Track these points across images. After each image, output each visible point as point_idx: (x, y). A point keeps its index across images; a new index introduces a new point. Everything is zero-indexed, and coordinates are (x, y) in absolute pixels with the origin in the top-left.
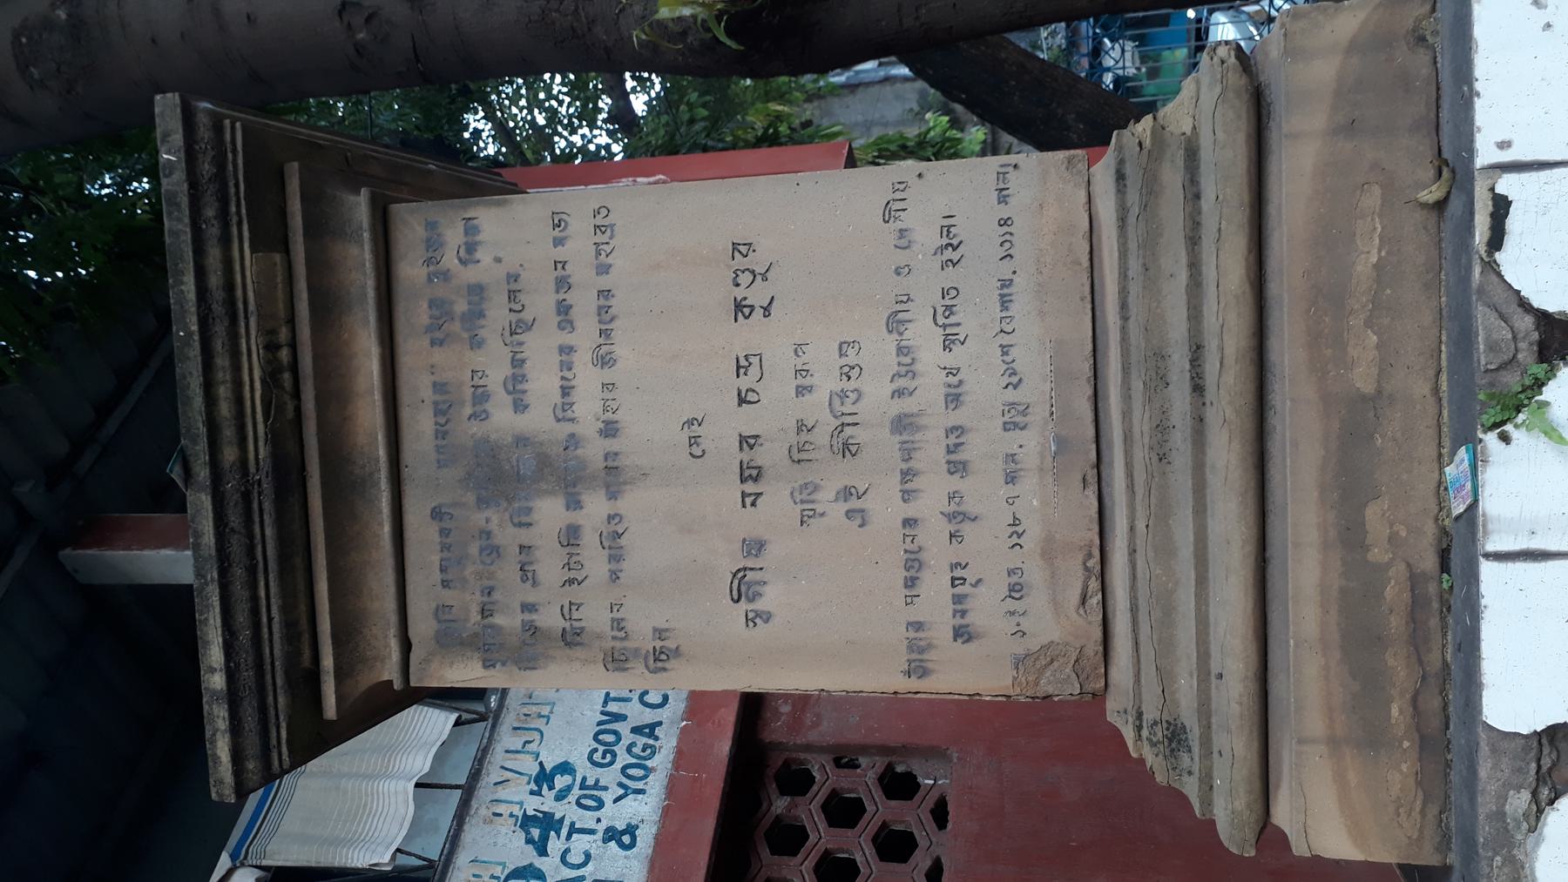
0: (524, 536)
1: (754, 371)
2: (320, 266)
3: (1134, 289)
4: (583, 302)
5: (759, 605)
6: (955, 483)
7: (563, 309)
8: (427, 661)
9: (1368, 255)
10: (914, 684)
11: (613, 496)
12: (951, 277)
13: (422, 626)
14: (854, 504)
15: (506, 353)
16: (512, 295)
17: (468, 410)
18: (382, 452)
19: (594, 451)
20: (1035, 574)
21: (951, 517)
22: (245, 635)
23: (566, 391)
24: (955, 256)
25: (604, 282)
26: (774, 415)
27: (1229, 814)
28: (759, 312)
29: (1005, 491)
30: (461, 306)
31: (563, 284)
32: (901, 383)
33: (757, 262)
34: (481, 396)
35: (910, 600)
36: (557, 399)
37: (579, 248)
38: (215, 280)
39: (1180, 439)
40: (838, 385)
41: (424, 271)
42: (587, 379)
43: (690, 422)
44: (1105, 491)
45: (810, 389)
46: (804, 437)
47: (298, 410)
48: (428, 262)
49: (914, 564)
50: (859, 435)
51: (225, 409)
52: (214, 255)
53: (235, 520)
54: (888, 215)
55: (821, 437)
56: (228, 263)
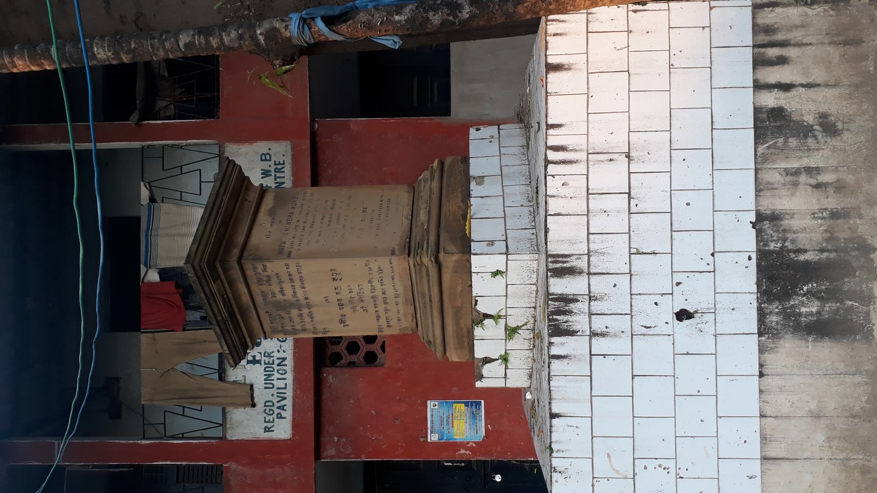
4: (296, 278)
7: (291, 280)
9: (459, 289)
19: (304, 302)
20: (402, 318)
22: (231, 343)
34: (273, 294)
38: (208, 292)
51: (216, 311)
52: (206, 288)
53: (223, 327)
56: (210, 288)
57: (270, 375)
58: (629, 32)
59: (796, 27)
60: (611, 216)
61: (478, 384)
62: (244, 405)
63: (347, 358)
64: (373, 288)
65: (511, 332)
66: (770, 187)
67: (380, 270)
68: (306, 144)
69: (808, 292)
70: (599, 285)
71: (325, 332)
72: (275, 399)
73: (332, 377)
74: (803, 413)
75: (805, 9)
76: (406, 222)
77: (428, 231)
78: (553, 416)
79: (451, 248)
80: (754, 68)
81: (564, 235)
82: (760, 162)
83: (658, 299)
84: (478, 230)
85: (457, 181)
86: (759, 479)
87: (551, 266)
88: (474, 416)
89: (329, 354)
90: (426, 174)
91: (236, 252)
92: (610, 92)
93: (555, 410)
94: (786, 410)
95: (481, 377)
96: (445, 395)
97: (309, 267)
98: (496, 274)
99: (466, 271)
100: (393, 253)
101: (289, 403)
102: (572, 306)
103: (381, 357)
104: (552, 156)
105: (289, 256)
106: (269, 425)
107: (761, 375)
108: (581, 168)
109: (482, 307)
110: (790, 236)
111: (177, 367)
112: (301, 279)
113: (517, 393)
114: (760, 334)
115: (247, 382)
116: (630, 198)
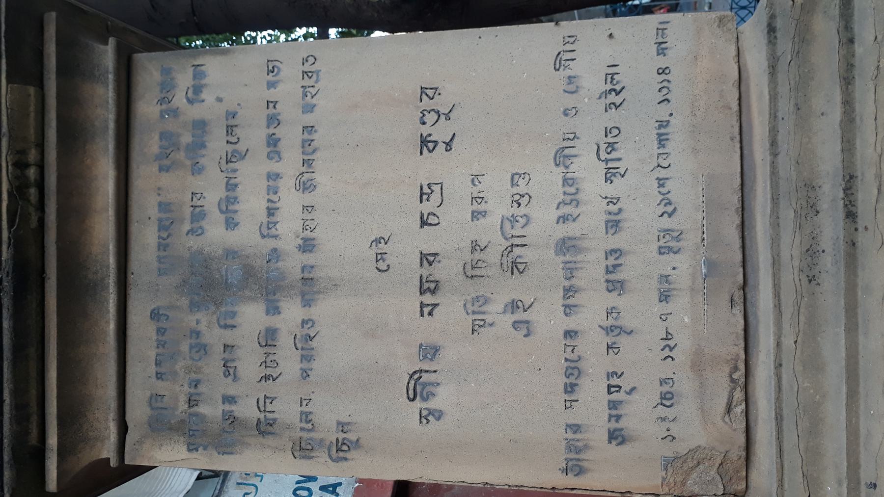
0: (229, 336)
1: (435, 198)
2: (69, 101)
3: (785, 128)
4: (290, 137)
5: (432, 404)
6: (613, 300)
7: (273, 142)
8: (140, 442)
10: (571, 481)
11: (307, 303)
12: (613, 118)
13: (137, 412)
14: (520, 316)
15: (221, 178)
16: (230, 130)
17: (187, 227)
18: (112, 260)
19: (293, 264)
20: (685, 385)
21: (609, 330)
23: (271, 212)
24: (618, 100)
25: (309, 119)
26: (452, 235)
28: (441, 147)
29: (659, 308)
30: (186, 138)
31: (273, 120)
32: (565, 210)
33: (442, 104)
34: (198, 215)
35: (569, 405)
36: (263, 217)
37: (288, 90)
39: (830, 263)
40: (508, 210)
41: (158, 108)
42: (290, 201)
43: (378, 241)
44: (749, 310)
45: (484, 214)
46: (477, 255)
47: (42, 222)
48: (161, 101)
49: (573, 371)
50: (527, 255)
54: (559, 63)
55: (493, 256)
67: (614, 91)
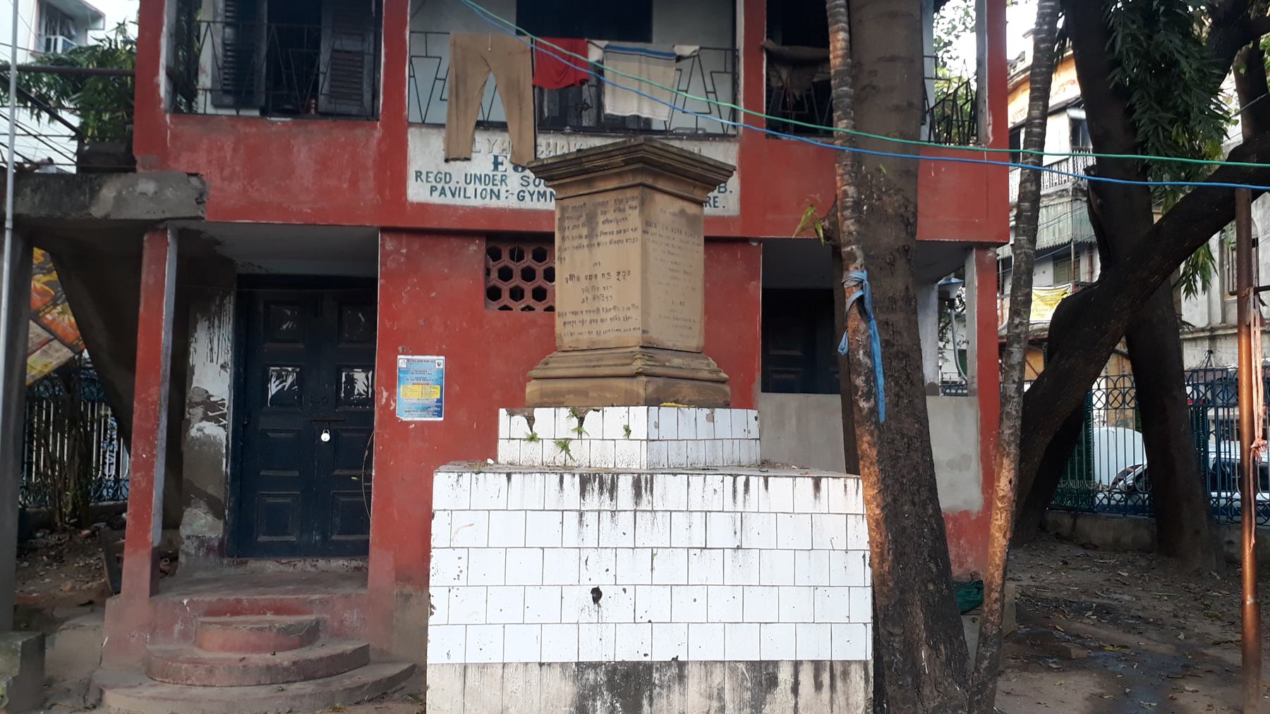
2: (626, 172)
4: (621, 237)
19: (595, 241)
20: (574, 337)
26: (601, 282)
27: (534, 373)
34: (605, 213)
49: (575, 313)
57: (480, 180)
58: (846, 551)
59: (847, 699)
60: (687, 531)
61: (503, 412)
62: (448, 149)
63: (495, 267)
64: (608, 310)
65: (564, 445)
66: (709, 674)
67: (628, 319)
68: (735, 232)
69: (615, 708)
70: (625, 519)
71: (560, 259)
72: (453, 185)
73: (475, 249)
74: (506, 702)
75: (863, 707)
76: (670, 345)
77: (664, 366)
78: (509, 476)
79: (651, 388)
80: (812, 661)
81: (669, 489)
82: (731, 665)
83: (612, 572)
84: (667, 414)
85: (713, 395)
86: (446, 661)
87: (643, 478)
88: (425, 409)
89: (500, 246)
90: (714, 365)
91: (649, 181)
92: (794, 533)
93: (513, 476)
94: (510, 687)
95: (511, 414)
96: (450, 377)
97: (633, 252)
98: (628, 430)
99: (629, 401)
100: (644, 332)
101: (448, 200)
102: (607, 495)
103: (495, 305)
104: (741, 480)
105: (645, 232)
106: (424, 177)
107: (541, 665)
108: (729, 505)
109: (591, 416)
110: (665, 692)
111: (491, 75)
112: (618, 242)
113: (492, 451)
114: (578, 664)
115: (474, 155)
116: (702, 549)
